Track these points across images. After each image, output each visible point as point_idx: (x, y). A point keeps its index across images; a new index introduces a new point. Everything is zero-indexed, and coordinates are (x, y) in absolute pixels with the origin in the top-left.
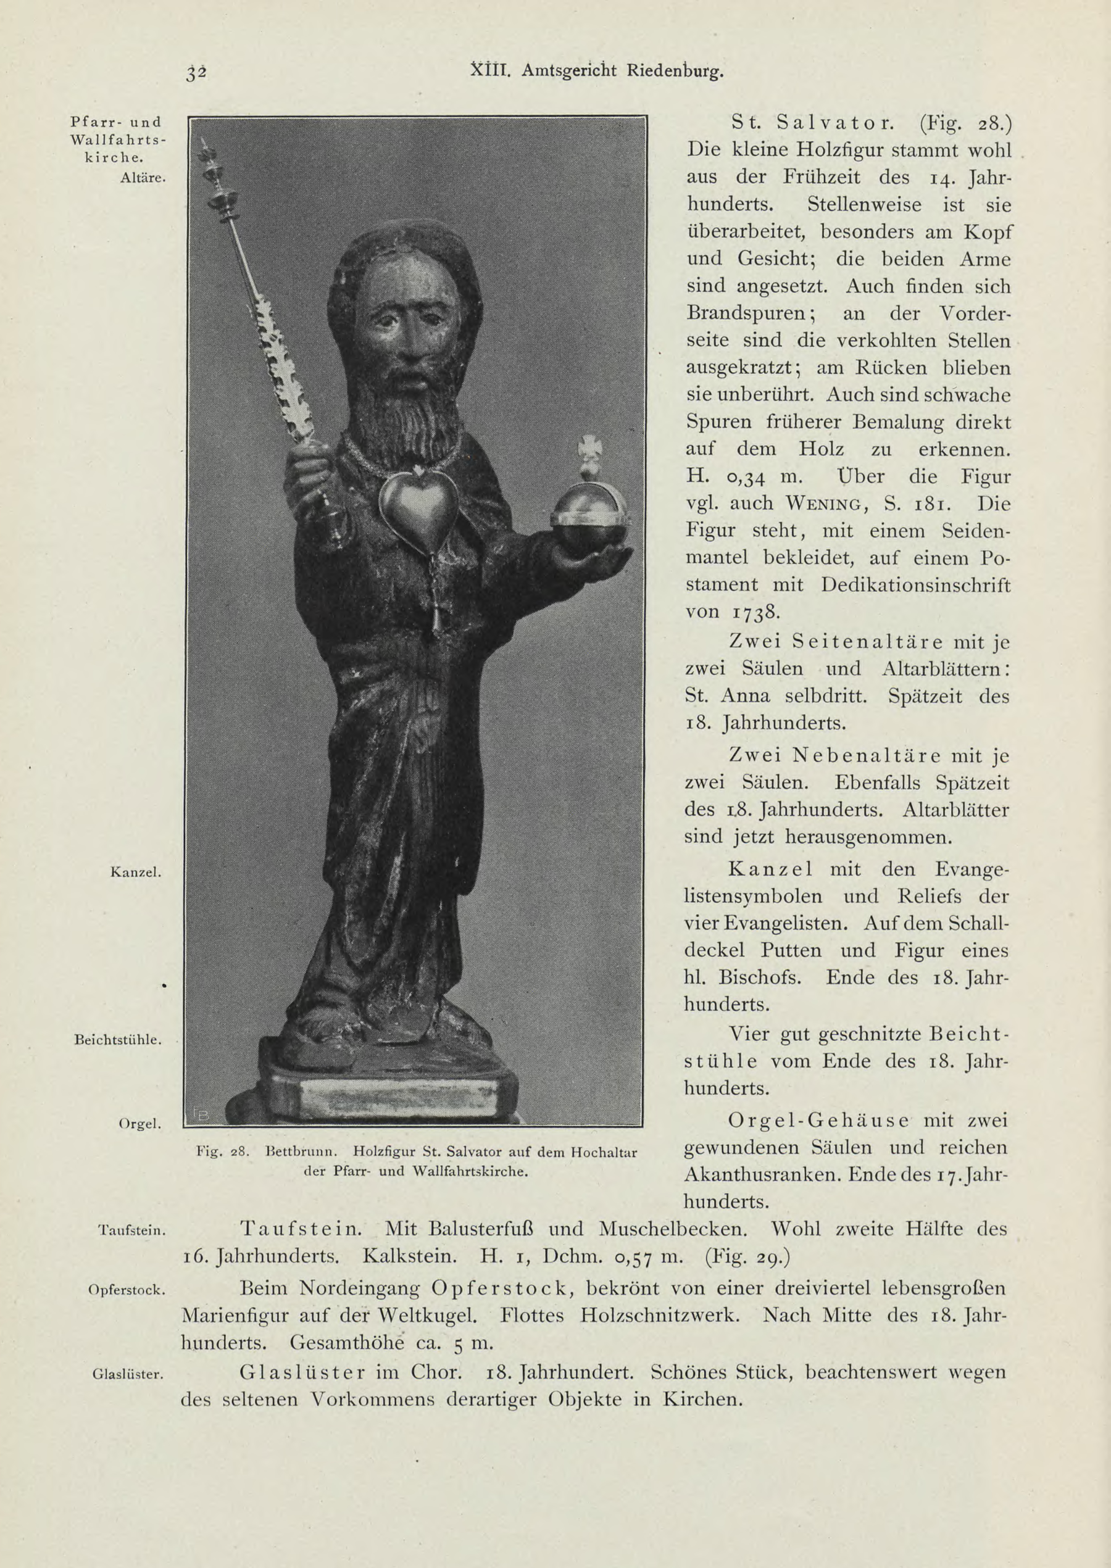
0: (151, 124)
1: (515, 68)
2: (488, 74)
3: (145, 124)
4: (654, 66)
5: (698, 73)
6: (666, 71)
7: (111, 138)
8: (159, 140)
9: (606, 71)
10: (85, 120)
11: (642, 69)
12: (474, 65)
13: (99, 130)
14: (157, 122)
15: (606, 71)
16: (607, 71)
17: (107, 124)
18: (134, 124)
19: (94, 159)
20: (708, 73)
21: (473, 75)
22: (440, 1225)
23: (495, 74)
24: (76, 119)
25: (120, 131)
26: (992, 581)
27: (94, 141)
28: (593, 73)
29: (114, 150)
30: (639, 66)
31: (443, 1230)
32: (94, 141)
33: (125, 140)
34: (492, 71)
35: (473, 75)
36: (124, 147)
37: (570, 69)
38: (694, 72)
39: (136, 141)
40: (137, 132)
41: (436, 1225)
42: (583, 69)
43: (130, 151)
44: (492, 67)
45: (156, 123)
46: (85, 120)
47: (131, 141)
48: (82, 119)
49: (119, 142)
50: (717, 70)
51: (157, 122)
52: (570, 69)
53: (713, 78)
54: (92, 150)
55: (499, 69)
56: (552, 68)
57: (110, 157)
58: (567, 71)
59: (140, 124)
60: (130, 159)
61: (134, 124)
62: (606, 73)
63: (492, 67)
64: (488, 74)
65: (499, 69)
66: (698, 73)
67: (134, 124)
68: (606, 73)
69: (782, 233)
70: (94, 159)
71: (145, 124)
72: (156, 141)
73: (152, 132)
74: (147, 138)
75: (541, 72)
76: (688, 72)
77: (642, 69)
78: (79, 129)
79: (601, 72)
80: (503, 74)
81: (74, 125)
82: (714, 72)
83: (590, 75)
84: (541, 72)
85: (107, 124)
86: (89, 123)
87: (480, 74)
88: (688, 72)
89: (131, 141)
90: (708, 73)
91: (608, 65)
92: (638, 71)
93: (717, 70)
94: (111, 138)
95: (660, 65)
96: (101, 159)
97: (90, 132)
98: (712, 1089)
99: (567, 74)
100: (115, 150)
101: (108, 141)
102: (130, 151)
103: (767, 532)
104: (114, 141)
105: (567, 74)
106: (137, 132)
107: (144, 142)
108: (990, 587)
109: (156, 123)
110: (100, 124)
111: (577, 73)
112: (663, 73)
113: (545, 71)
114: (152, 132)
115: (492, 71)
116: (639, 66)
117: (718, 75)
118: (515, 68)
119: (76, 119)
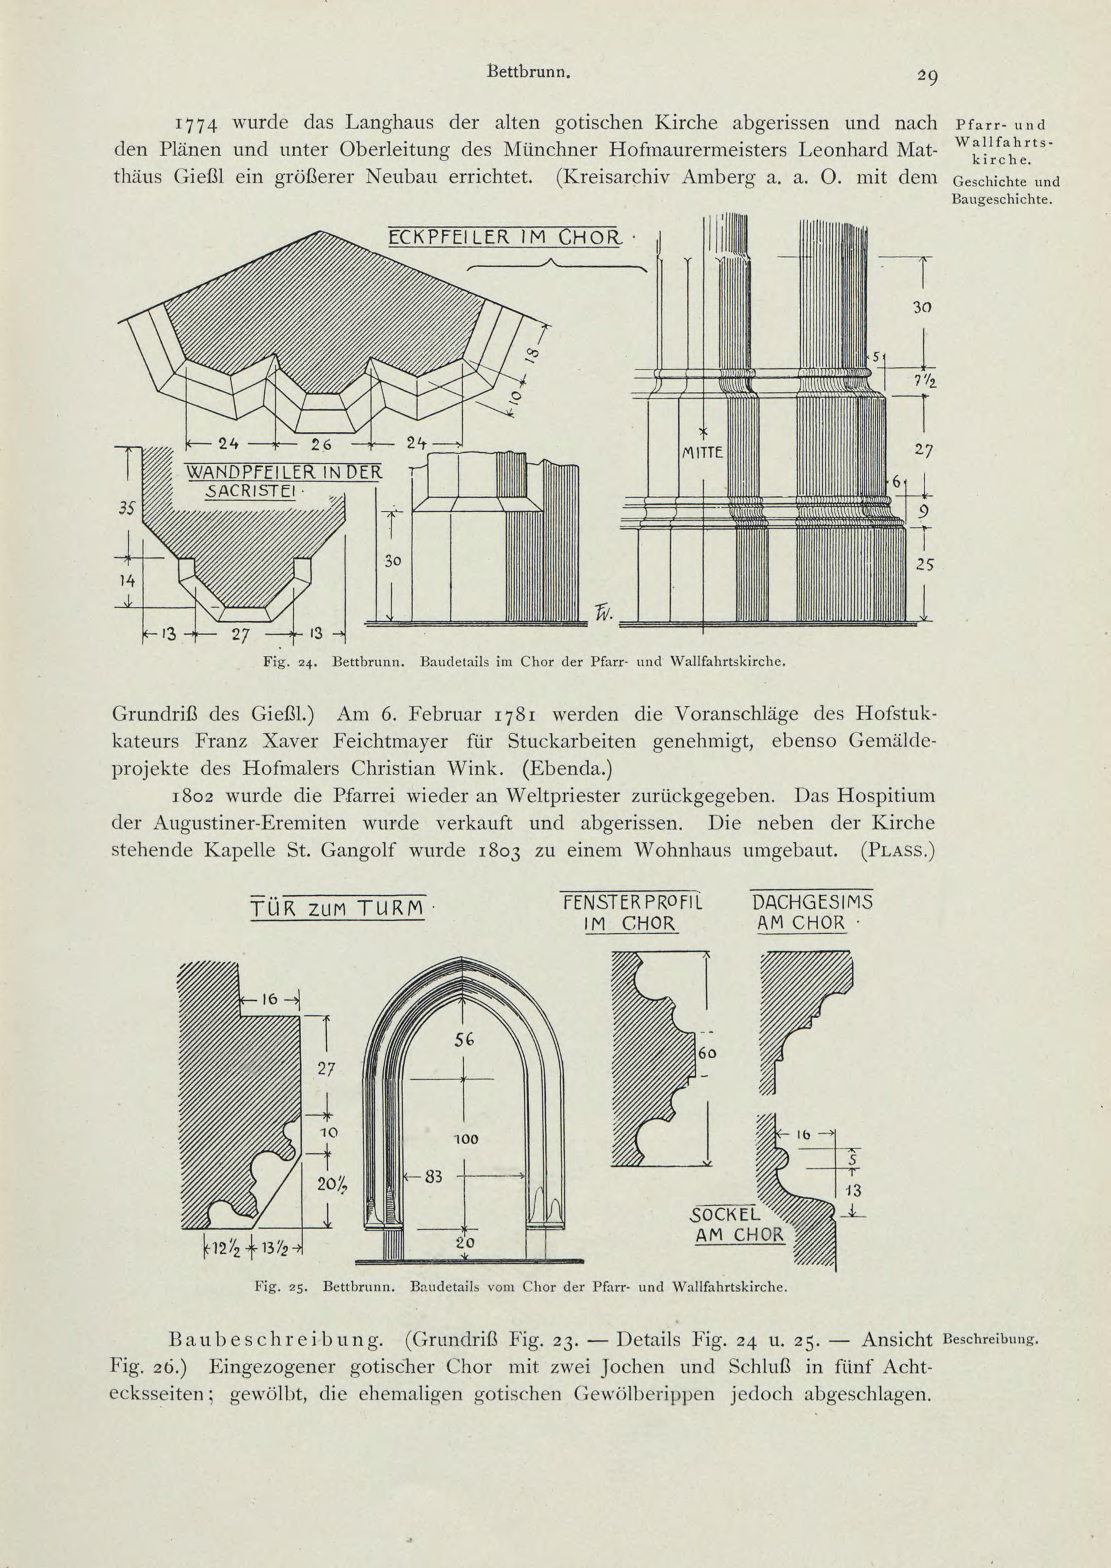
3: (1030, 126)
7: (998, 141)
8: (1047, 143)
10: (970, 124)
13: (984, 132)
14: (1042, 125)
17: (992, 127)
18: (1018, 126)
19: (981, 161)
25: (1008, 134)
27: (981, 143)
29: (1003, 152)
32: (981, 143)
33: (1012, 143)
36: (1012, 150)
39: (1023, 144)
40: (1024, 135)
43: (1018, 153)
45: (1041, 126)
46: (970, 124)
48: (967, 122)
51: (1042, 125)
54: (980, 152)
57: (998, 159)
59: (1024, 126)
60: (1018, 161)
61: (1019, 127)
67: (1019, 127)
70: (981, 161)
71: (1030, 126)
73: (1036, 134)
74: (1035, 141)
78: (964, 131)
85: (992, 127)
86: (974, 126)
94: (998, 141)
96: (989, 161)
97: (978, 135)
100: (1004, 152)
101: (995, 143)
102: (1018, 153)
104: (1001, 143)
106: (1024, 135)
107: (1031, 144)
109: (1041, 126)
110: (984, 126)
114: (1036, 134)
119: (961, 122)
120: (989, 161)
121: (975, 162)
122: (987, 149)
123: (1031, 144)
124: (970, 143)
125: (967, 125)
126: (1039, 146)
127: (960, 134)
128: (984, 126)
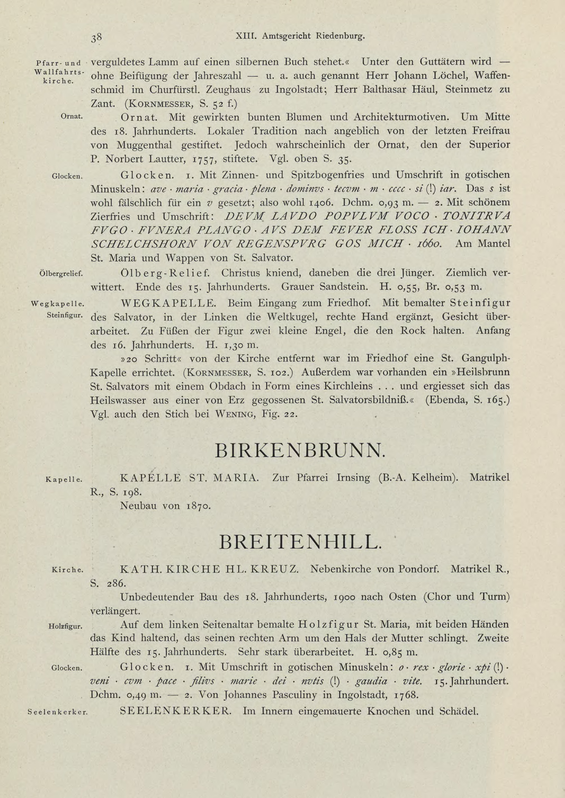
0: (75, 64)
1: (259, 34)
2: (245, 38)
3: (73, 64)
4: (330, 33)
5: (352, 37)
6: (335, 36)
7: (56, 71)
8: (81, 73)
9: (305, 36)
10: (44, 63)
11: (324, 35)
12: (238, 33)
13: (51, 67)
15: (305, 36)
16: (306, 36)
17: (54, 64)
19: (48, 82)
20: (357, 37)
21: (237, 38)
22: (206, 595)
23: (249, 38)
24: (39, 62)
25: (61, 68)
26: (258, 665)
27: (48, 72)
28: (299, 37)
29: (58, 77)
30: (322, 34)
31: (207, 598)
32: (48, 72)
33: (63, 72)
34: (247, 37)
35: (237, 38)
37: (286, 35)
38: (349, 36)
39: (69, 73)
40: (70, 68)
41: (204, 595)
42: (293, 35)
43: (67, 78)
44: (247, 35)
45: (78, 64)
46: (44, 63)
47: (66, 73)
48: (42, 62)
49: (61, 73)
50: (361, 35)
51: (79, 63)
52: (286, 35)
53: (360, 39)
54: (47, 77)
55: (250, 36)
56: (277, 35)
58: (285, 36)
59: (70, 64)
61: (67, 64)
62: (305, 37)
63: (247, 35)
64: (245, 38)
65: (250, 36)
66: (352, 37)
68: (305, 37)
69: (383, 118)
70: (48, 82)
71: (73, 64)
72: (79, 73)
73: (76, 68)
74: (75, 71)
75: (272, 37)
76: (347, 37)
77: (324, 35)
79: (302, 37)
80: (252, 38)
81: (38, 65)
82: (360, 36)
83: (297, 38)
84: (272, 37)
85: (54, 64)
86: (45, 64)
87: (241, 38)
88: (347, 37)
89: (66, 73)
90: (357, 37)
91: (306, 33)
92: (322, 36)
93: (361, 35)
94: (56, 71)
95: (333, 33)
96: (52, 81)
97: (46, 68)
98: (298, 597)
99: (284, 38)
100: (59, 77)
101: (55, 72)
102: (67, 78)
103: (350, 287)
104: (58, 72)
105: (284, 38)
106: (70, 68)
107: (73, 73)
108: (257, 668)
109: (78, 64)
110: (50, 64)
111: (290, 37)
112: (334, 37)
113: (274, 36)
114: (76, 68)
115: (247, 37)
116: (322, 34)
117: (362, 38)
118: (259, 34)
119: (39, 62)
120: (52, 81)
121: (45, 82)
122: (51, 76)
123: (73, 73)
124: (42, 72)
125: (42, 63)
126: (77, 74)
127: (37, 68)
128: (50, 64)
